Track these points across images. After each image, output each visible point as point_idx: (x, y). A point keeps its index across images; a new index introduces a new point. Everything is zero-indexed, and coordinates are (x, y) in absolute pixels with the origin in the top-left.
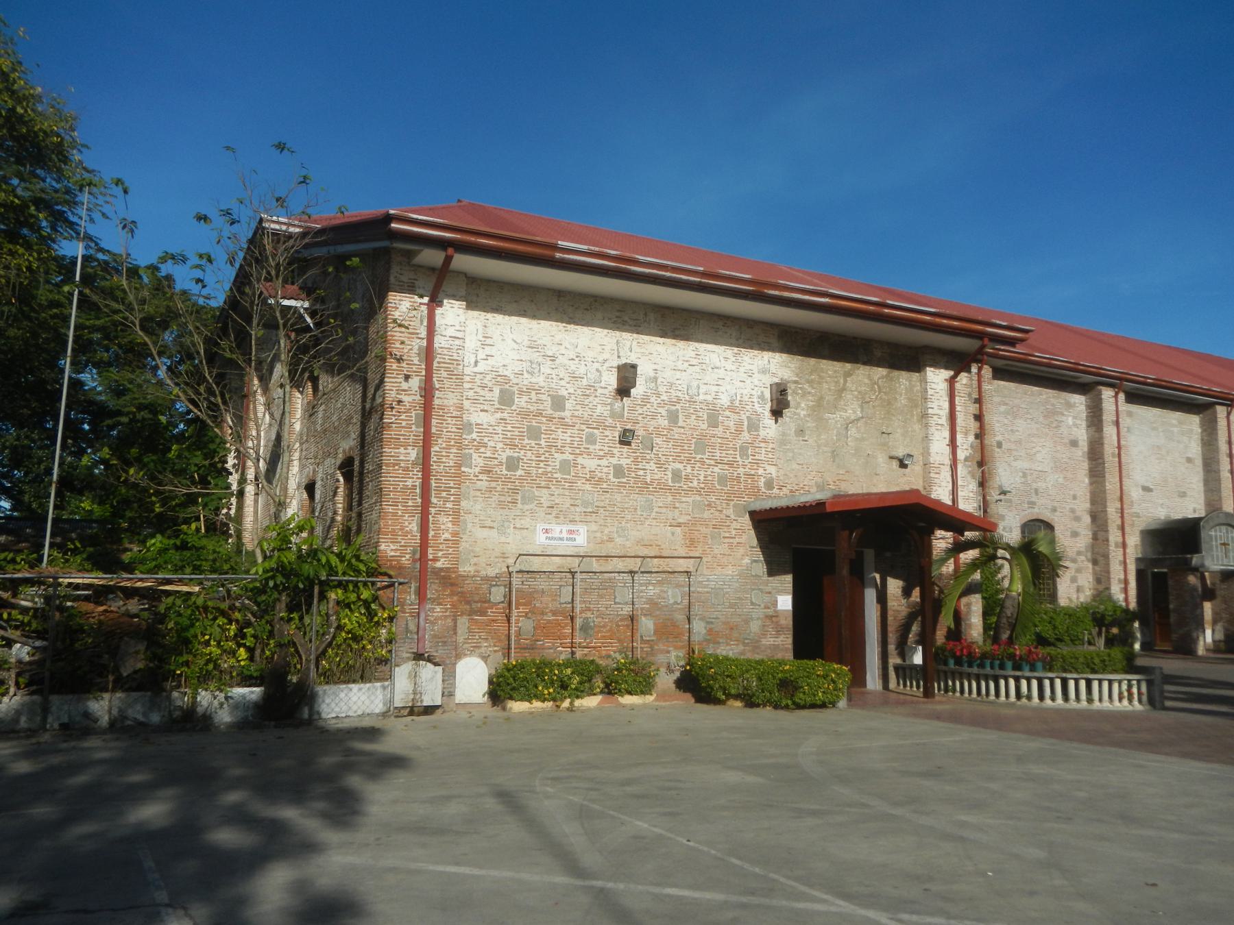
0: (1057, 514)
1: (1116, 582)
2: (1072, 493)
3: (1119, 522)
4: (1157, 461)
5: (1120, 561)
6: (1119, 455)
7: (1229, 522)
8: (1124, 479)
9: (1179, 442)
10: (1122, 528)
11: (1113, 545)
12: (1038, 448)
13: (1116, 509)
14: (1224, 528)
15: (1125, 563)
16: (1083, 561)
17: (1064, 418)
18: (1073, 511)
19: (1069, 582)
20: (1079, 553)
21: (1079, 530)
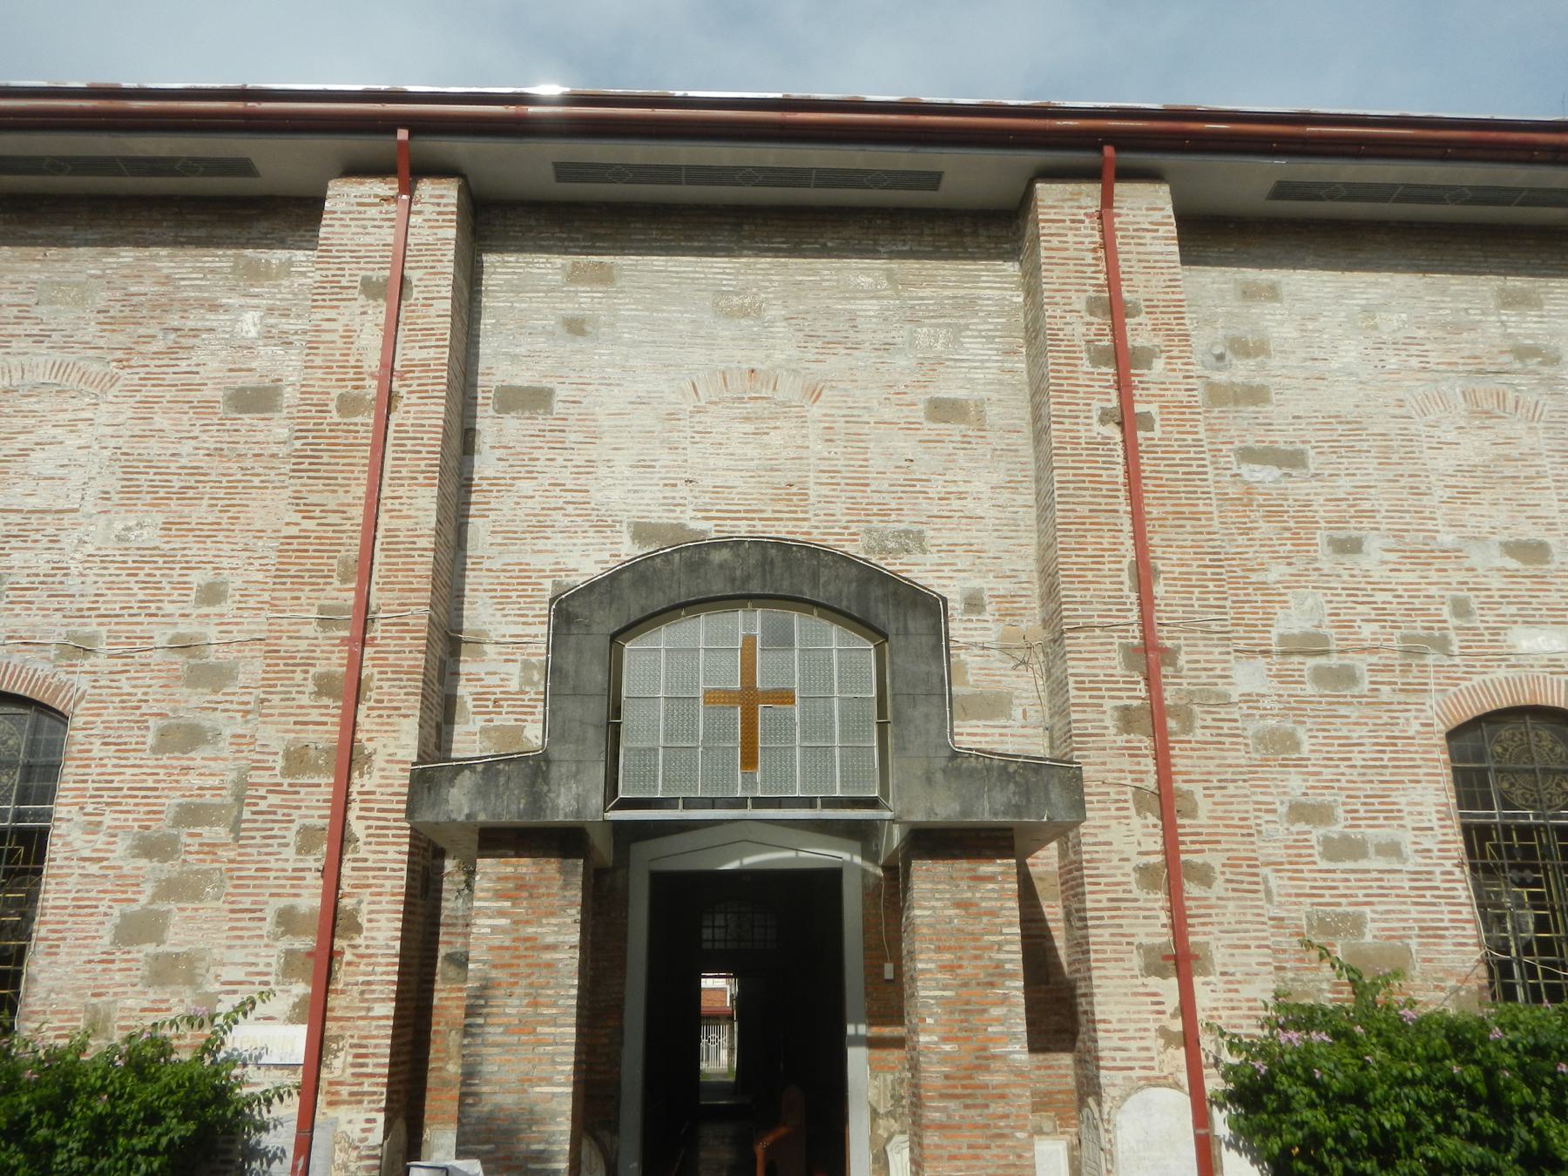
0: (101, 662)
1: (268, 926)
2: (197, 578)
3: (335, 663)
4: (749, 428)
5: (305, 831)
6: (389, 400)
7: (785, 588)
8: (386, 491)
9: (887, 347)
10: (355, 690)
11: (280, 763)
12: (47, 432)
13: (321, 610)
14: (748, 623)
15: (341, 839)
16: (211, 848)
17: (213, 319)
18: (184, 646)
19: (107, 940)
20: (191, 814)
21: (207, 720)
